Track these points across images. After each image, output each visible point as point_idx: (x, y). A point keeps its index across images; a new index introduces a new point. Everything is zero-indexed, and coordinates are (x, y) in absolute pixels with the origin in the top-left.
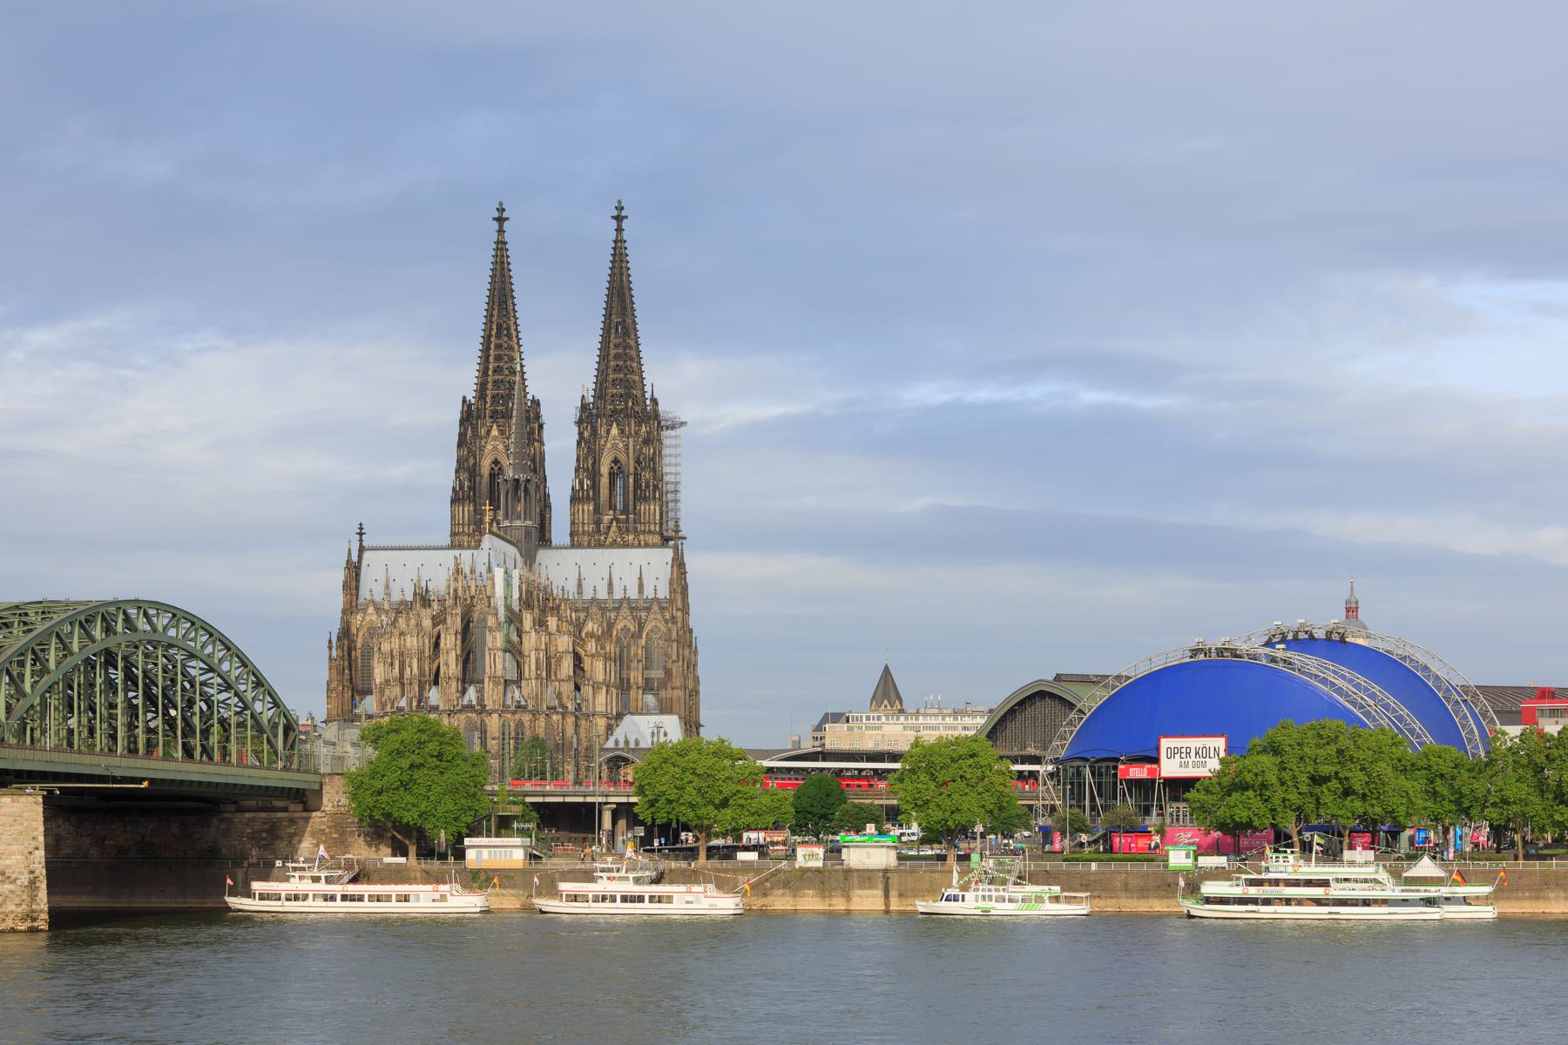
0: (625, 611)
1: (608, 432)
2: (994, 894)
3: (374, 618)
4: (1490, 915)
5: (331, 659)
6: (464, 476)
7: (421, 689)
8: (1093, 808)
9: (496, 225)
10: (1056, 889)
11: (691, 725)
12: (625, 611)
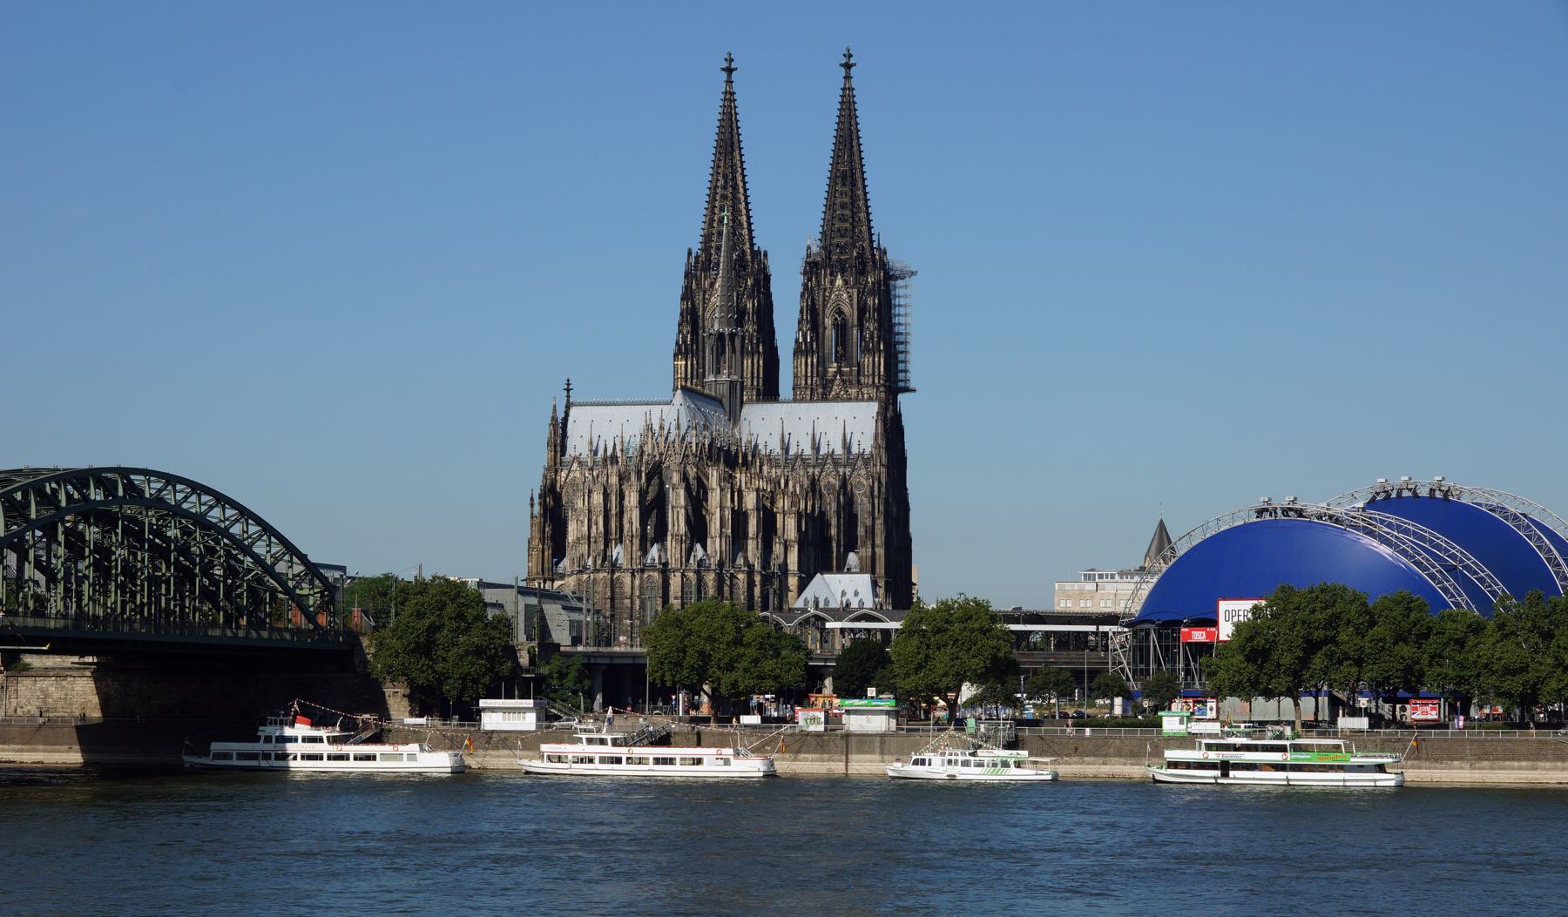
0: (829, 467)
1: (832, 282)
4: (1392, 783)
6: (687, 329)
7: (606, 546)
9: (724, 75)
11: (897, 582)
12: (829, 467)
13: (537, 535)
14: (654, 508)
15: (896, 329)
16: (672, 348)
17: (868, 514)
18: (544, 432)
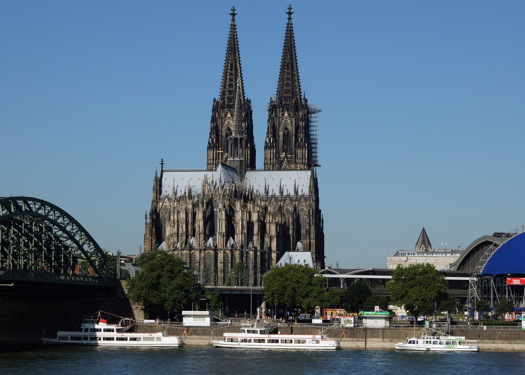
0: (288, 201)
1: (283, 115)
2: (432, 340)
3: (168, 204)
5: (146, 224)
6: (214, 136)
8: (495, 299)
10: (463, 338)
12: (288, 201)
13: (148, 232)
14: (210, 220)
15: (312, 137)
16: (207, 145)
17: (303, 224)
18: (152, 183)
